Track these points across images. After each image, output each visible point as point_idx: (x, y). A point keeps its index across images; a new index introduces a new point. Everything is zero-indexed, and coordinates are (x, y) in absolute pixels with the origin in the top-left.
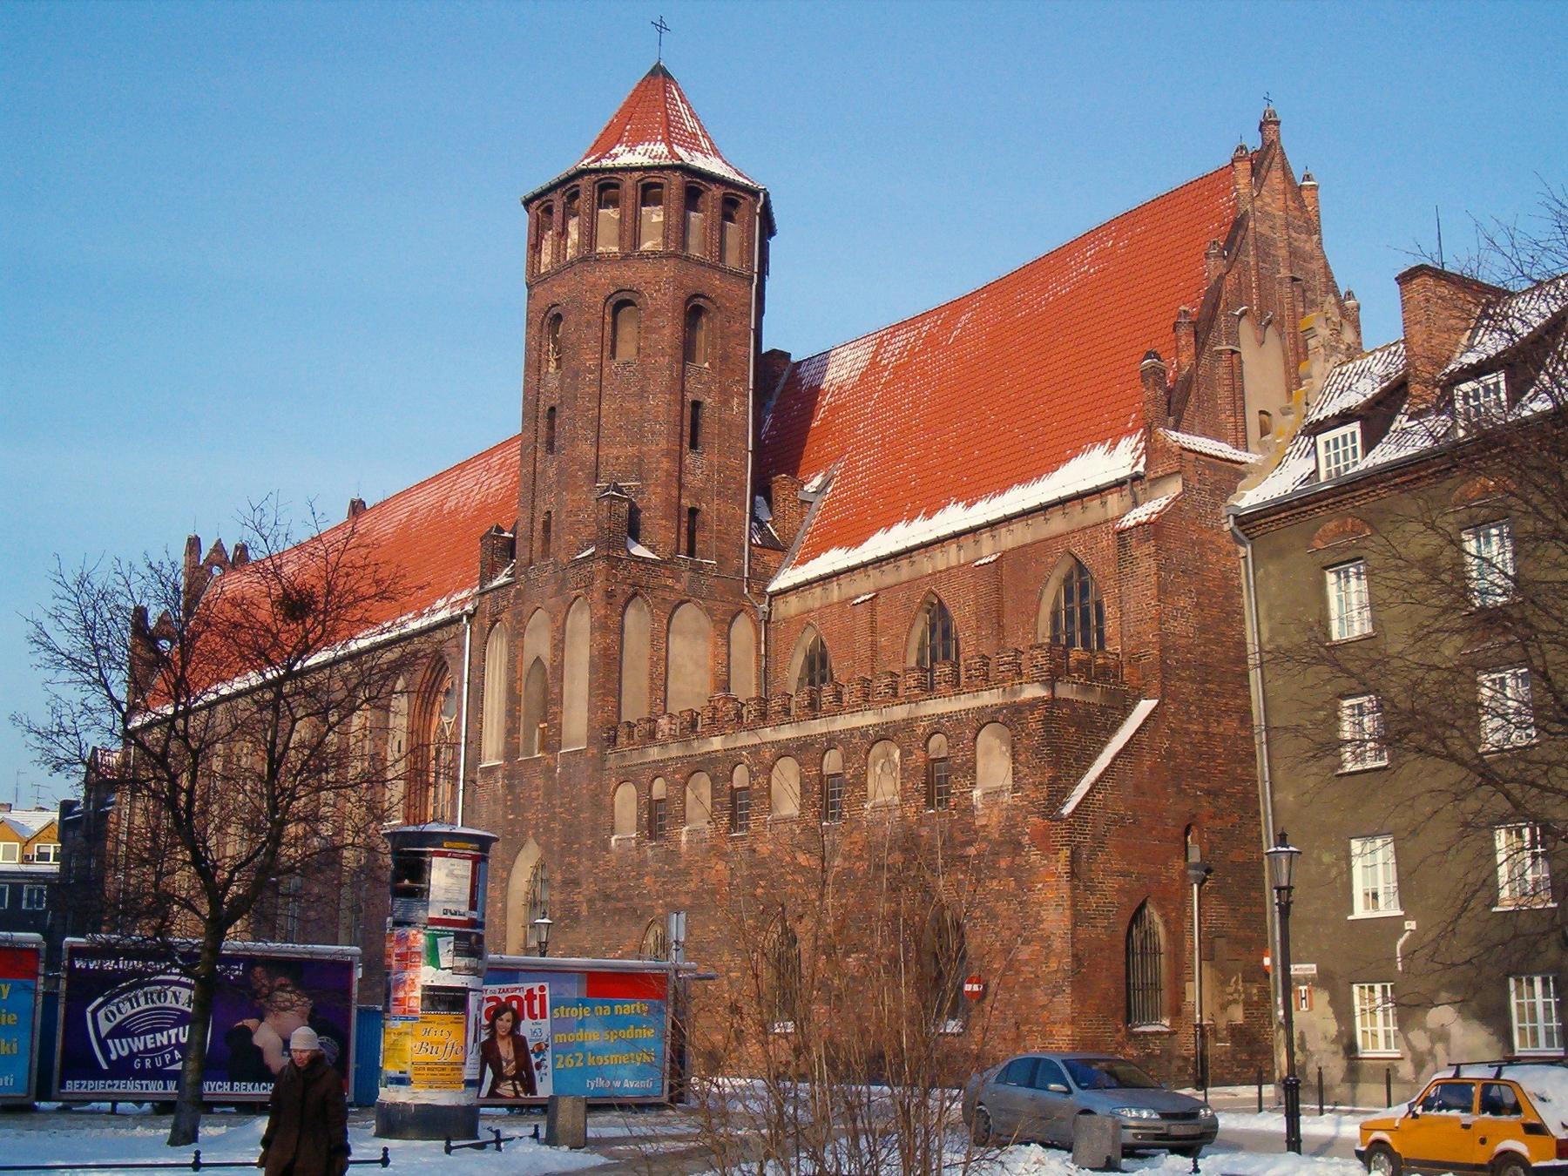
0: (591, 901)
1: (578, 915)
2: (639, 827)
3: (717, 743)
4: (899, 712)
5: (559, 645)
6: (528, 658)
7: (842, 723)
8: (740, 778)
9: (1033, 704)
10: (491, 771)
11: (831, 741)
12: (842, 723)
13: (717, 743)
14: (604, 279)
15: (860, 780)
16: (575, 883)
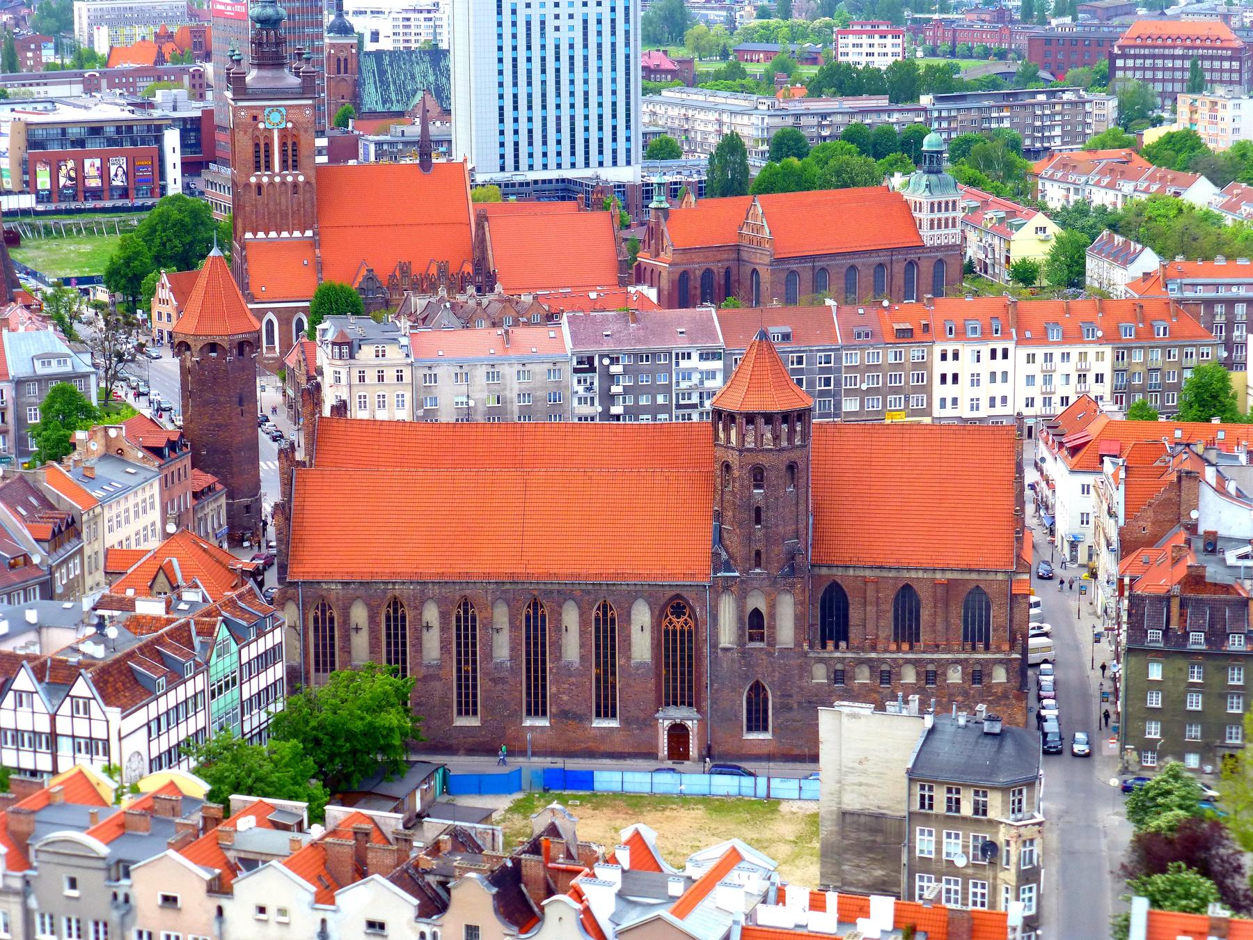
0: (800, 703)
1: (791, 709)
2: (828, 678)
3: (873, 655)
4: (962, 656)
5: (772, 606)
6: (750, 608)
7: (935, 656)
8: (885, 667)
9: (1016, 659)
10: (726, 650)
11: (932, 661)
12: (935, 656)
13: (873, 655)
14: (786, 457)
15: (944, 674)
16: (790, 696)
